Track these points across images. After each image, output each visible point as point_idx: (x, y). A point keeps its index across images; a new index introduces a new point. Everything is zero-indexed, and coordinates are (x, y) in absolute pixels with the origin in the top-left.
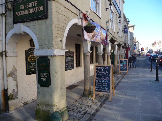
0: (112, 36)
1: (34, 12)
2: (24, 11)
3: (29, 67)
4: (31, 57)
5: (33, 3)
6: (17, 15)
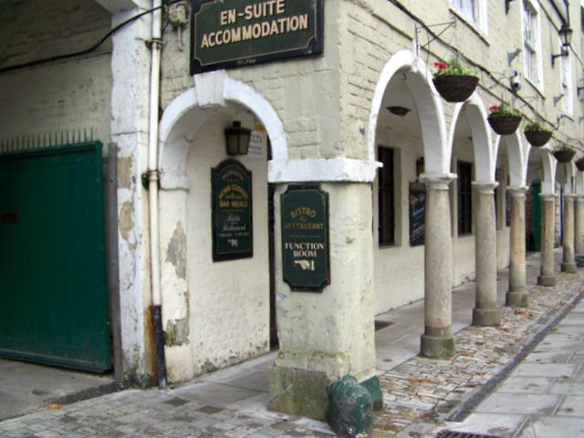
0: (447, 56)
1: (274, 33)
2: (247, 29)
3: (221, 233)
4: (229, 193)
5: (268, 3)
6: (206, 42)
